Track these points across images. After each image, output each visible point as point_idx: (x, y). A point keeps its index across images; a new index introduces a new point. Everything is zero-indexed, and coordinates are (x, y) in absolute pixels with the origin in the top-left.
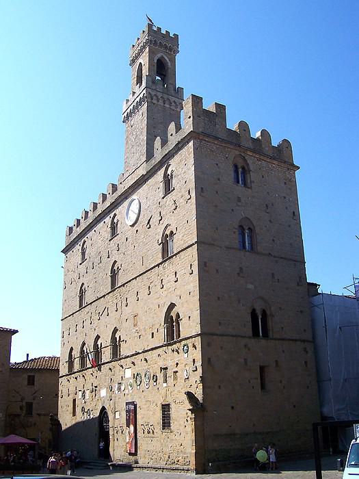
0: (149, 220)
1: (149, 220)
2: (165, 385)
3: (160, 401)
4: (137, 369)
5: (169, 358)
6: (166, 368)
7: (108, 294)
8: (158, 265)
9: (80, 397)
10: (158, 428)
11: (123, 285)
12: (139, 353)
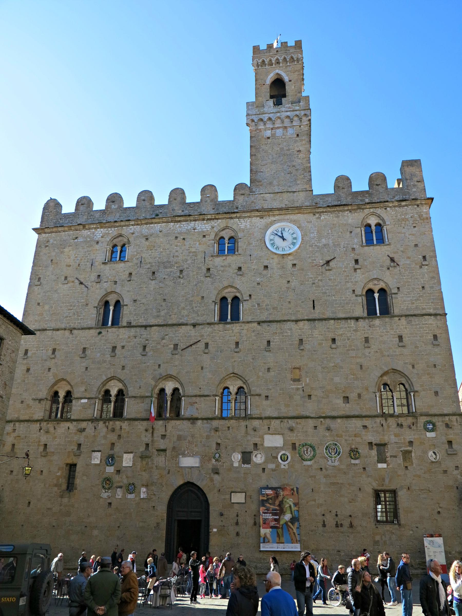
0: (328, 262)
1: (328, 262)
2: (380, 466)
3: (369, 485)
6: (385, 445)
7: (209, 324)
8: (357, 319)
9: (96, 461)
11: (259, 323)
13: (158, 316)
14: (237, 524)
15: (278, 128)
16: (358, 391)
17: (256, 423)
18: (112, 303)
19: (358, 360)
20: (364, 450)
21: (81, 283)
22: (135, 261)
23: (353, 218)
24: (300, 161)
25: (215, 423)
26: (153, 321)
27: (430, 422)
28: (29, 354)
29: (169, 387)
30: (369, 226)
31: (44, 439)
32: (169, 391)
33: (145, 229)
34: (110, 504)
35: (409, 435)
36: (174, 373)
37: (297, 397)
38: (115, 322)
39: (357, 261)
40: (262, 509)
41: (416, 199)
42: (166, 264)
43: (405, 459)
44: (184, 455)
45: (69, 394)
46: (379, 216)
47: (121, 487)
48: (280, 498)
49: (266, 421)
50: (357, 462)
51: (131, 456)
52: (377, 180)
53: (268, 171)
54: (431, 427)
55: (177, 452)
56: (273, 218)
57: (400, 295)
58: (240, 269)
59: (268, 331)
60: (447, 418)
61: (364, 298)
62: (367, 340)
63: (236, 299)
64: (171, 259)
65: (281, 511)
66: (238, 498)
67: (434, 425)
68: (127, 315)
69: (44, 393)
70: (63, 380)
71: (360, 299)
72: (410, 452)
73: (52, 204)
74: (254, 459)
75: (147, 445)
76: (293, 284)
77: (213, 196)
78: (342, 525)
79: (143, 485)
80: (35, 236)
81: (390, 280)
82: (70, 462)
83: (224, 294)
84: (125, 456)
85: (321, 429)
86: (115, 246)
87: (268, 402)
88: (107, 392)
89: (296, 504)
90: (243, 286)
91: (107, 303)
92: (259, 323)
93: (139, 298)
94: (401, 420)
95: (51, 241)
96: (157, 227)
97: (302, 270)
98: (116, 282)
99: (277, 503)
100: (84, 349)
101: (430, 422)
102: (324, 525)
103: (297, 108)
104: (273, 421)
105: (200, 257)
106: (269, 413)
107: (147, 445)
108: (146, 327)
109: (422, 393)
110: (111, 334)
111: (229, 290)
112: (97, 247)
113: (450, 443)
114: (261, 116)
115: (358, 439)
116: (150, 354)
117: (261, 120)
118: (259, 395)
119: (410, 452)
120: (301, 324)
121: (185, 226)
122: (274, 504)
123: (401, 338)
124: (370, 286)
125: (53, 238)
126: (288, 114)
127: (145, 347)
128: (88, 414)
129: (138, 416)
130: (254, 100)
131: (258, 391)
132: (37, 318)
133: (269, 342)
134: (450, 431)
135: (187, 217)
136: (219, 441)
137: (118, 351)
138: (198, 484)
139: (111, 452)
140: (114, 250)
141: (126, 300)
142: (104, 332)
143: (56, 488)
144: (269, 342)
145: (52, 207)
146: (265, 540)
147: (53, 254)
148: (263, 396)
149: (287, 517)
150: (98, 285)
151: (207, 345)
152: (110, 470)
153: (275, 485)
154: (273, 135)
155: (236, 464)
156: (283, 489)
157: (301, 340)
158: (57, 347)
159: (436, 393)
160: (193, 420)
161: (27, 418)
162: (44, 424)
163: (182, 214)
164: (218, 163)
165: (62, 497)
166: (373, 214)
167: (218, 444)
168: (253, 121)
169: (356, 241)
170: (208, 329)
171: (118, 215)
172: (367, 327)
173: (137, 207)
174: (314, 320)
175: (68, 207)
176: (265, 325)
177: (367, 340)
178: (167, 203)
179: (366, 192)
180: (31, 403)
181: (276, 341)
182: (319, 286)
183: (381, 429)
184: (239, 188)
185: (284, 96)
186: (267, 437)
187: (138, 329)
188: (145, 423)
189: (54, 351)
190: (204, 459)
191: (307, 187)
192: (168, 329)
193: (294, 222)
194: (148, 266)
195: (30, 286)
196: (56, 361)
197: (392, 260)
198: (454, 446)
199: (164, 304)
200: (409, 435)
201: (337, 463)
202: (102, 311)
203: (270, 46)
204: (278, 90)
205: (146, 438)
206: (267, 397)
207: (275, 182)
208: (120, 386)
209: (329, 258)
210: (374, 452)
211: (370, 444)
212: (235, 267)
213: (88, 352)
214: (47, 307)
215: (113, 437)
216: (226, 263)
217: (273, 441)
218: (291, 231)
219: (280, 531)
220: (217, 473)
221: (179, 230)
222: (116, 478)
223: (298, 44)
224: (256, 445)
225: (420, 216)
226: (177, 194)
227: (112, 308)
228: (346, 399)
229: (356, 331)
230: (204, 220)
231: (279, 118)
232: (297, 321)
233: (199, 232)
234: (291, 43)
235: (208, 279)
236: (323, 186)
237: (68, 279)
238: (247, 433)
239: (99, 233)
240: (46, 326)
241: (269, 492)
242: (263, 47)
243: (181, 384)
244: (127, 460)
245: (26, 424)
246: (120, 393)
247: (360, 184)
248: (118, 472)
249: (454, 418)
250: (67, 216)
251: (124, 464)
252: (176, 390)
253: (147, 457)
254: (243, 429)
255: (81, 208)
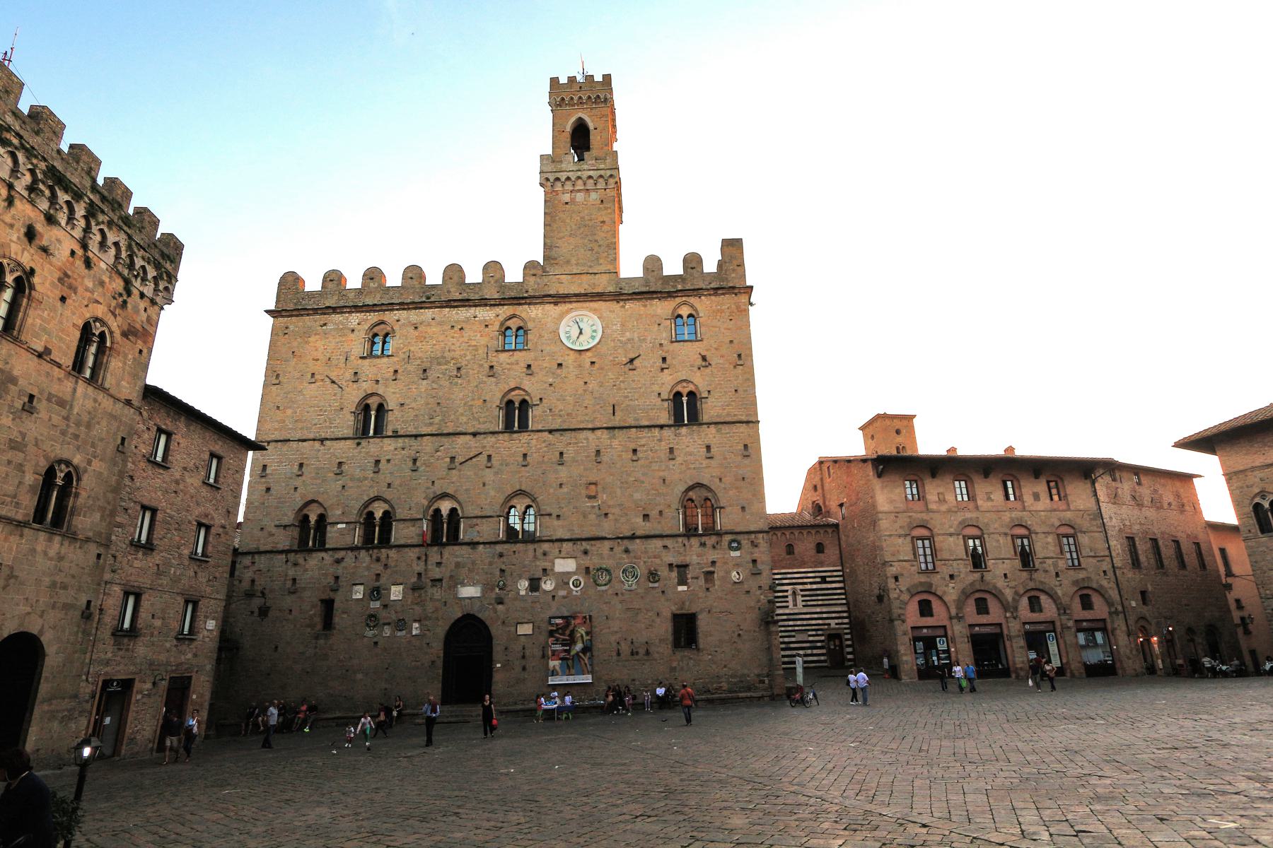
0: (632, 361)
1: (632, 361)
2: (681, 588)
3: (668, 609)
4: (593, 561)
5: (695, 554)
6: (686, 566)
8: (662, 427)
10: (665, 649)
11: (550, 431)
12: (605, 538)
13: (431, 424)
14: (524, 657)
15: (579, 191)
16: (659, 508)
17: (546, 546)
18: (374, 406)
19: (662, 474)
20: (663, 572)
21: (333, 382)
22: (402, 356)
23: (662, 308)
24: (603, 235)
25: (499, 548)
26: (425, 430)
27: (734, 541)
28: (268, 471)
29: (445, 507)
30: (680, 316)
31: (291, 573)
32: (445, 512)
33: (414, 316)
34: (376, 643)
35: (713, 555)
36: (449, 491)
37: (592, 517)
38: (378, 431)
39: (664, 359)
40: (551, 640)
41: (734, 288)
42: (441, 360)
43: (706, 581)
44: (463, 585)
45: (322, 518)
46: (692, 306)
47: (389, 624)
48: (571, 628)
49: (557, 544)
50: (656, 585)
51: (401, 588)
52: (692, 262)
53: (564, 248)
54: (735, 545)
55: (455, 582)
56: (569, 306)
57: (709, 400)
58: (529, 366)
59: (560, 442)
60: (753, 536)
61: (671, 404)
62: (671, 450)
63: (524, 402)
64: (447, 354)
65: (572, 641)
66: (525, 629)
67: (739, 543)
68: (394, 421)
69: (289, 517)
70: (313, 501)
71: (666, 404)
72: (713, 573)
73: (290, 279)
74: (543, 586)
75: (419, 574)
76: (590, 386)
77: (498, 276)
78: (637, 653)
79: (415, 621)
80: (270, 320)
81: (700, 381)
82: (324, 597)
83: (510, 397)
84: (393, 588)
85: (619, 549)
86: (376, 335)
87: (560, 523)
88: (371, 515)
89: (587, 633)
90: (533, 388)
91: (367, 408)
92: (550, 431)
93: (407, 402)
94: (703, 539)
95: (292, 327)
96: (428, 314)
97: (602, 369)
98: (377, 381)
99: (568, 632)
100: (340, 463)
101: (734, 541)
102: (619, 654)
103: (602, 166)
104: (565, 544)
105: (482, 351)
106: (560, 535)
107: (419, 574)
108: (416, 436)
109: (728, 509)
110: (374, 447)
111: (517, 392)
112: (352, 336)
113: (754, 561)
114: (558, 175)
115: (658, 561)
116: (421, 469)
117: (558, 179)
118: (550, 515)
119: (713, 573)
120: (599, 433)
121: (463, 313)
122: (563, 634)
123: (708, 448)
124: (679, 388)
125: (295, 323)
126: (591, 173)
127: (415, 461)
128: (347, 541)
129: (409, 542)
130: (550, 151)
131: (549, 510)
132: (276, 425)
133: (561, 454)
134: (756, 550)
135: (465, 303)
136: (503, 567)
137: (383, 465)
138: (480, 616)
139: (377, 584)
140: (377, 340)
141: (391, 404)
142: (364, 443)
143: (309, 630)
144: (561, 454)
145: (290, 282)
146: (554, 673)
147: (295, 344)
148: (554, 516)
149: (579, 646)
150: (355, 385)
151: (489, 456)
152: (377, 604)
153: (566, 614)
154: (573, 200)
155: (523, 593)
156: (574, 618)
157: (598, 452)
158: (305, 462)
159: (743, 508)
160: (473, 544)
161: (268, 548)
162: (292, 556)
163: (460, 297)
164: (506, 233)
165: (317, 638)
166: (685, 303)
167: (502, 571)
168: (547, 179)
169: (664, 335)
170: (491, 439)
171: (378, 296)
172: (672, 437)
173: (402, 287)
174: (614, 428)
175: (313, 284)
176: (557, 435)
177: (671, 450)
178: (440, 282)
179: (680, 276)
180: (274, 530)
181: (570, 453)
182: (620, 389)
183: (682, 550)
184: (530, 267)
185: (588, 149)
186: (557, 561)
187: (407, 440)
188: (417, 550)
189: (301, 465)
190: (487, 587)
191: (610, 267)
192: (444, 439)
193: (595, 311)
194: (418, 362)
195: (265, 386)
196: (304, 478)
197: (704, 358)
198: (760, 566)
199: (438, 409)
200: (713, 555)
201: (634, 587)
202: (361, 417)
203: (572, 80)
204: (580, 138)
205: (420, 567)
206: (558, 516)
207: (573, 261)
208: (386, 507)
209: (633, 356)
210: (674, 574)
211: (670, 565)
212: (523, 365)
213: (345, 467)
214: (289, 412)
215: (378, 568)
216: (513, 359)
217: (565, 565)
218: (591, 322)
219: (570, 663)
220: (501, 603)
221: (456, 317)
222: (383, 614)
223: (607, 78)
224: (545, 570)
225: (738, 307)
226: (454, 272)
227: (373, 413)
228: (646, 517)
229: (660, 440)
230: (486, 305)
231: (579, 178)
232: (593, 429)
233: (480, 322)
234: (598, 78)
235: (492, 379)
236: (630, 268)
237: (317, 377)
238: (535, 557)
239: (354, 319)
240: (289, 437)
241: (559, 621)
242: (563, 80)
243: (459, 502)
244: (396, 593)
245: (268, 556)
246: (387, 515)
247: (673, 267)
248: (385, 606)
249: (761, 535)
250: (312, 295)
251: (392, 598)
252: (453, 511)
253: (420, 588)
254: (531, 553)
255: (330, 285)
